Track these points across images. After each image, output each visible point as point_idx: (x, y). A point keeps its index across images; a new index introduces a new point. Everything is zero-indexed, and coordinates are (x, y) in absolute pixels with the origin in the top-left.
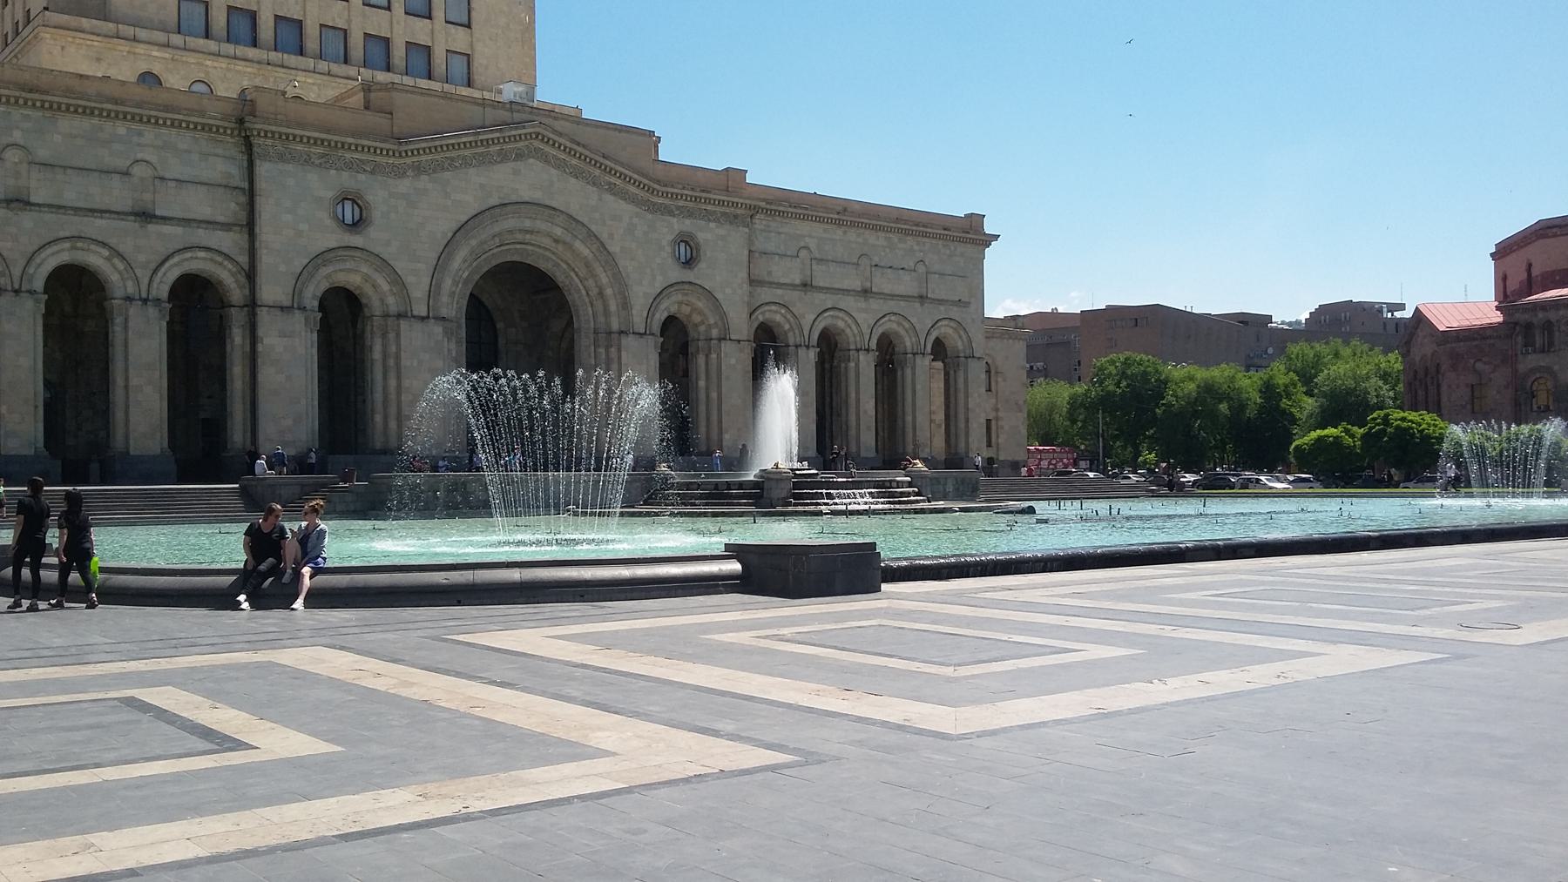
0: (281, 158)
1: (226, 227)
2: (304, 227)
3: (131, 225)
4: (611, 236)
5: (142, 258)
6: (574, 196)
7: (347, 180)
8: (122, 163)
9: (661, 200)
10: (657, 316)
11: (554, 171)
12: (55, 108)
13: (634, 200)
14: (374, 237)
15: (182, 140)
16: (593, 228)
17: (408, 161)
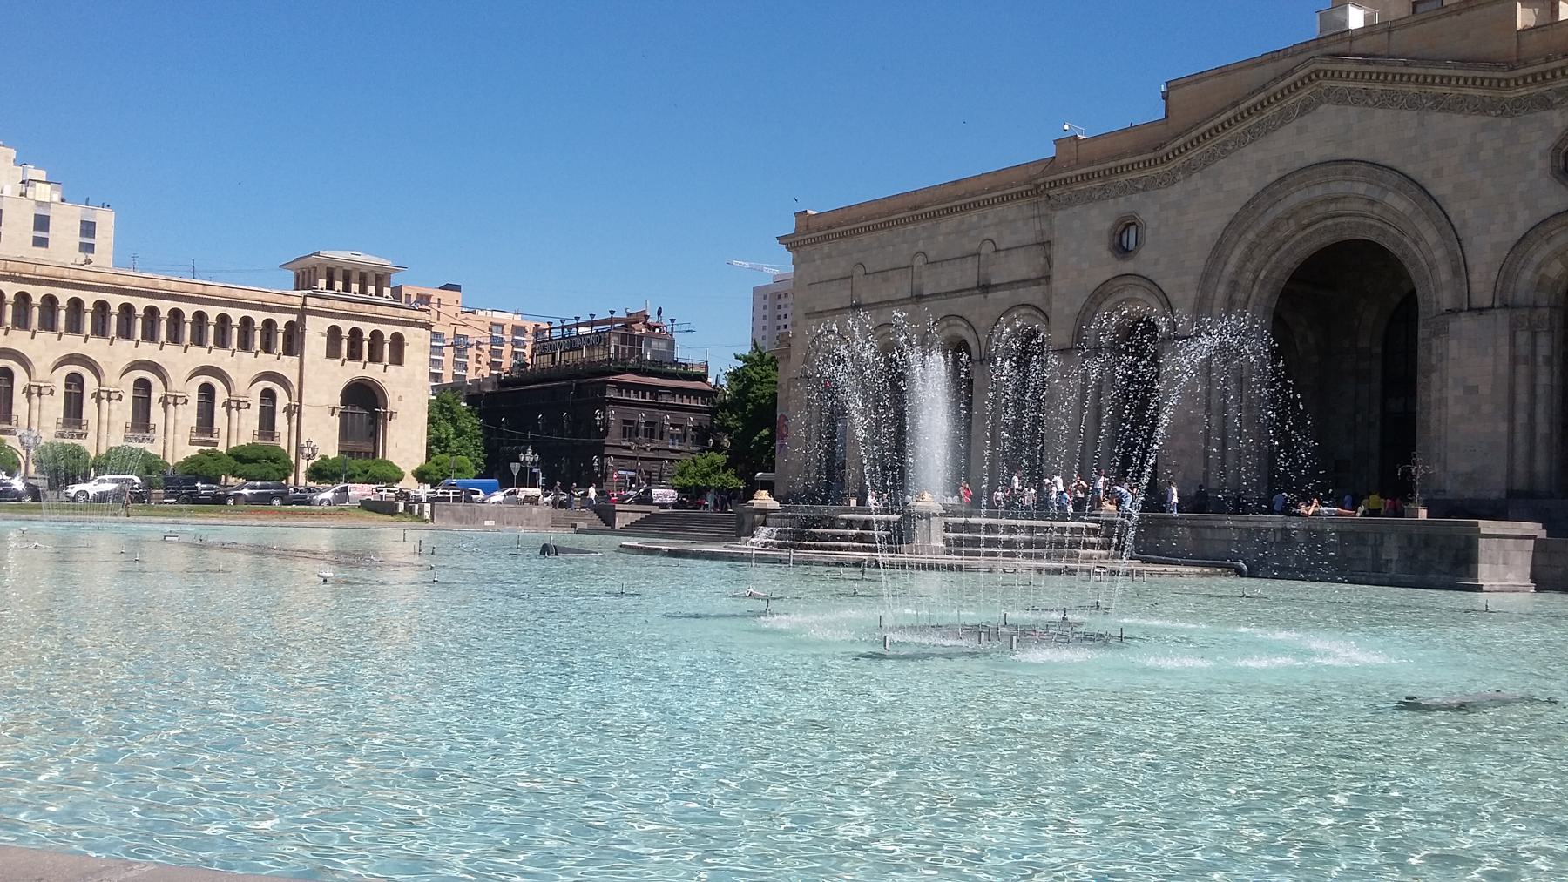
0: (1069, 202)
1: (1035, 281)
2: (1085, 266)
3: (978, 297)
4: (1438, 173)
5: (983, 324)
6: (1379, 132)
7: (1121, 206)
8: (974, 246)
9: (1523, 92)
10: (1528, 274)
11: (1352, 110)
12: (933, 216)
13: (1482, 108)
14: (1145, 261)
15: (1010, 211)
16: (1410, 170)
17: (1178, 162)
